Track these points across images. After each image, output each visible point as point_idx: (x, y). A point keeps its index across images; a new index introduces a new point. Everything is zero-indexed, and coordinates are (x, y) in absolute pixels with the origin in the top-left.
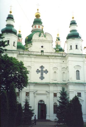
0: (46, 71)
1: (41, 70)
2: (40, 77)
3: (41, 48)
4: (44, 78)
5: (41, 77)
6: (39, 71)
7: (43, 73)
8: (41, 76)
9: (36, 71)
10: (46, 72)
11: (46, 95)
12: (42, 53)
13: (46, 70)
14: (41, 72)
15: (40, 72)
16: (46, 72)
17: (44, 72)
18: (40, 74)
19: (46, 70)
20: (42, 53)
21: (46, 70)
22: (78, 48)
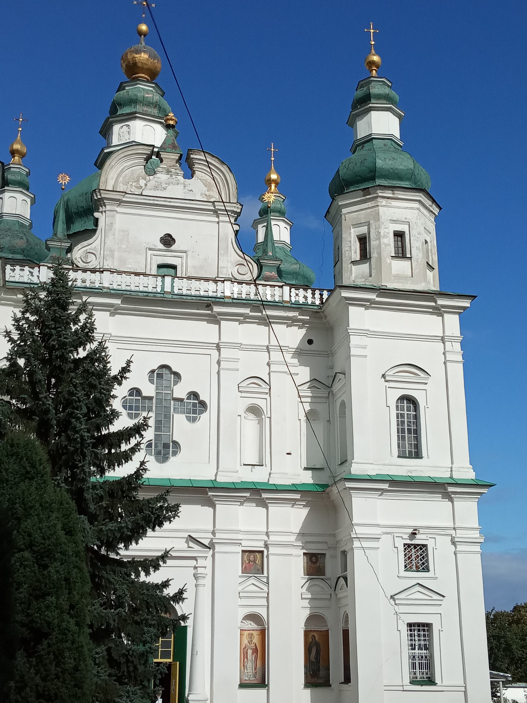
3: (161, 246)
7: (168, 417)
11: (193, 563)
13: (194, 395)
20: (168, 280)
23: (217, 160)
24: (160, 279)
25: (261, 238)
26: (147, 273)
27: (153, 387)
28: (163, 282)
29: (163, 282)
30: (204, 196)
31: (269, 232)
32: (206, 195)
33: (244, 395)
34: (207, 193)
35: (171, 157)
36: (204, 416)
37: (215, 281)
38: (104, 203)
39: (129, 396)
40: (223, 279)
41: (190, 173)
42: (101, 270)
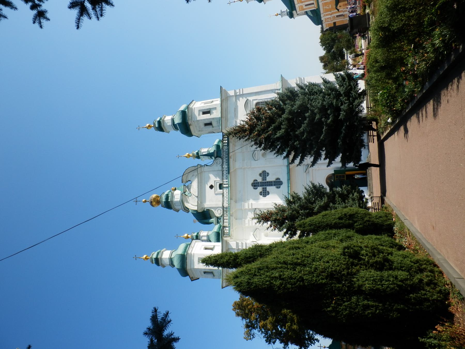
0: (263, 176)
1: (261, 186)
2: (277, 187)
3: (214, 189)
4: (277, 179)
6: (263, 190)
7: (268, 182)
8: (274, 185)
9: (264, 196)
10: (264, 174)
12: (225, 186)
13: (260, 175)
15: (266, 188)
16: (264, 174)
17: (264, 178)
19: (260, 175)
21: (261, 176)
22: (209, 110)
27: (259, 188)
28: (225, 187)
33: (259, 158)
34: (195, 176)
37: (223, 171)
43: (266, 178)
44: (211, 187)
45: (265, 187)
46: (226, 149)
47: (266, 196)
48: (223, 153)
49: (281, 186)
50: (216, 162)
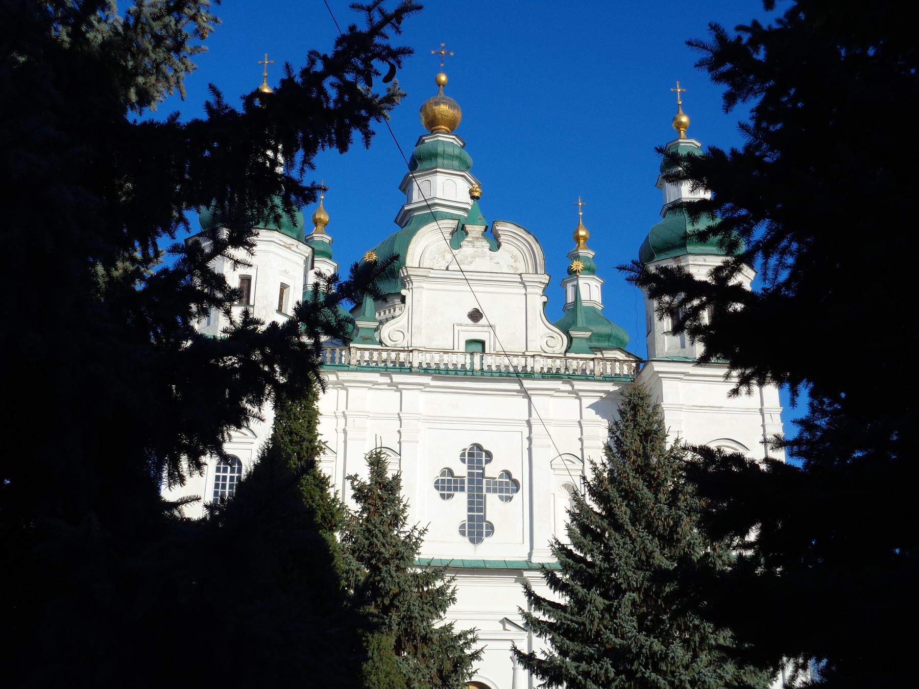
1: (470, 474)
2: (463, 526)
3: (470, 322)
4: (491, 527)
5: (470, 526)
7: (480, 497)
8: (470, 518)
9: (437, 482)
12: (477, 358)
14: (471, 489)
15: (462, 489)
18: (461, 499)
20: (477, 358)
21: (501, 476)
23: (522, 230)
24: (468, 356)
25: (570, 298)
26: (456, 350)
27: (465, 466)
28: (472, 359)
29: (472, 359)
30: (510, 267)
31: (578, 298)
32: (512, 266)
33: (557, 472)
34: (514, 264)
35: (475, 230)
36: (517, 497)
38: (411, 280)
39: (441, 476)
40: (532, 354)
41: (496, 245)
42: (410, 349)
43: (495, 491)
44: (476, 316)
45: (466, 488)
46: (592, 371)
47: (437, 488)
48: (582, 359)
49: (466, 539)
50: (555, 335)
